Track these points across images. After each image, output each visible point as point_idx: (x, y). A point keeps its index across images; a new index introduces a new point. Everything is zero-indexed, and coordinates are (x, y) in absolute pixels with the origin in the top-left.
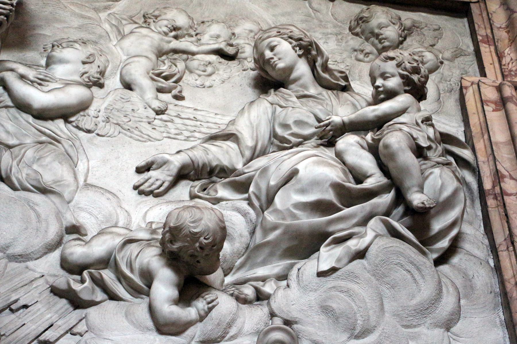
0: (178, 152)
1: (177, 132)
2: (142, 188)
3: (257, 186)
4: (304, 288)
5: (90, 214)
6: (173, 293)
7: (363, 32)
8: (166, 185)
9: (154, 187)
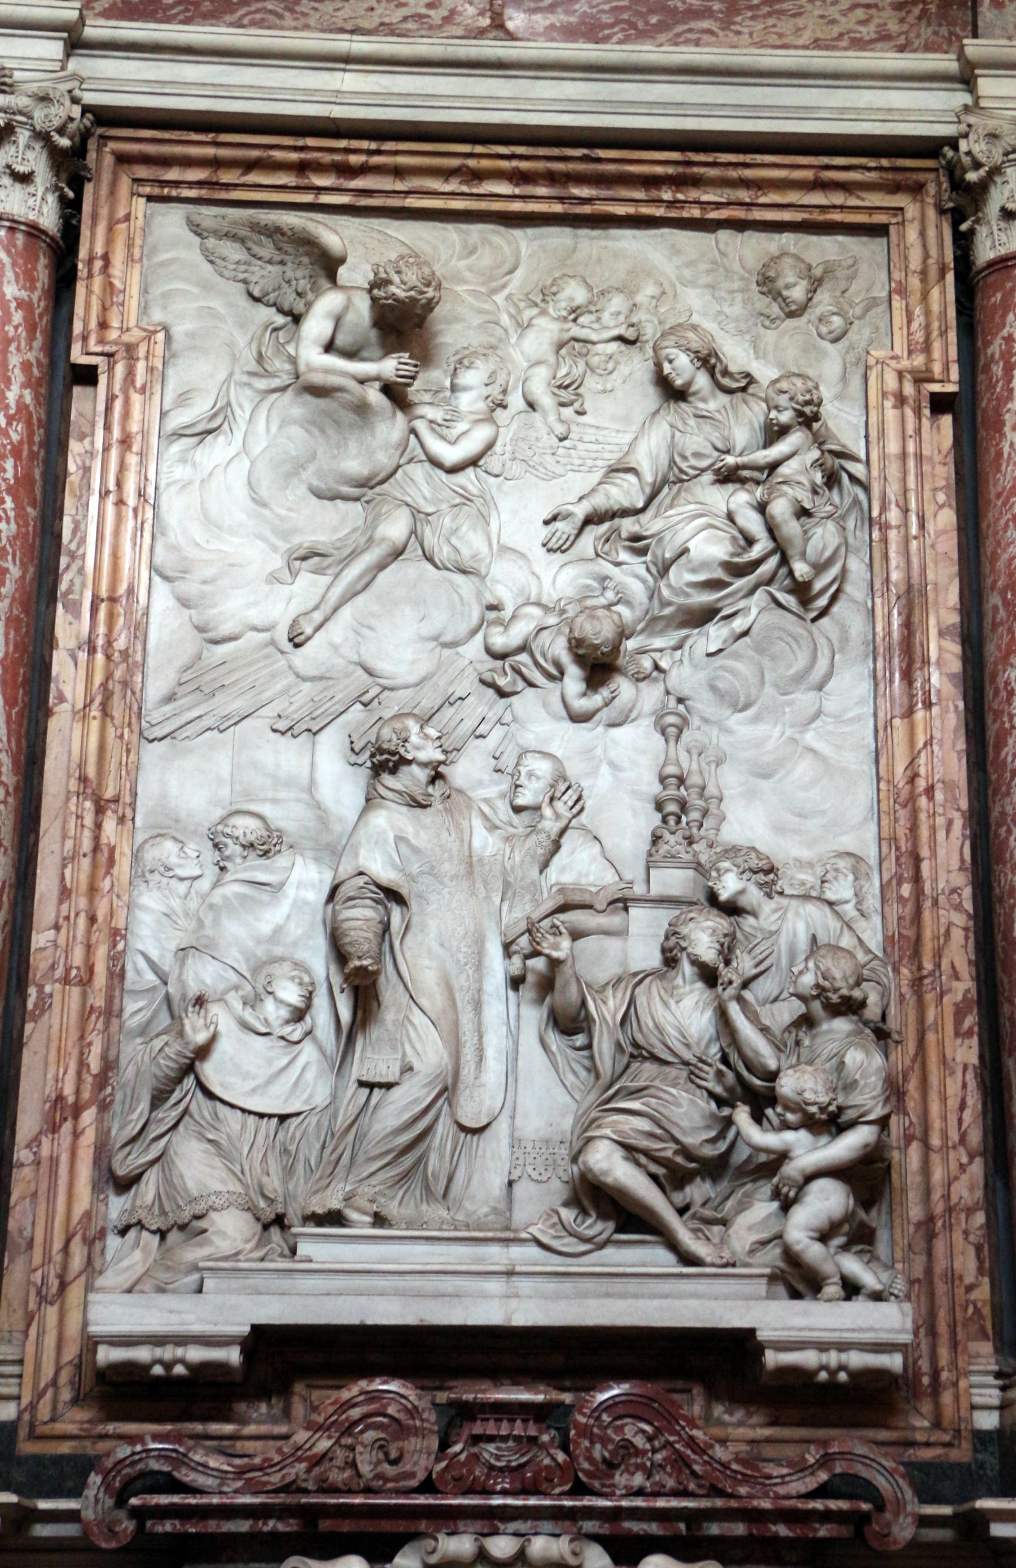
0: (581, 499)
1: (580, 462)
2: (550, 545)
3: (654, 555)
4: (695, 667)
5: (506, 586)
6: (581, 686)
7: (770, 292)
8: (572, 538)
9: (561, 542)
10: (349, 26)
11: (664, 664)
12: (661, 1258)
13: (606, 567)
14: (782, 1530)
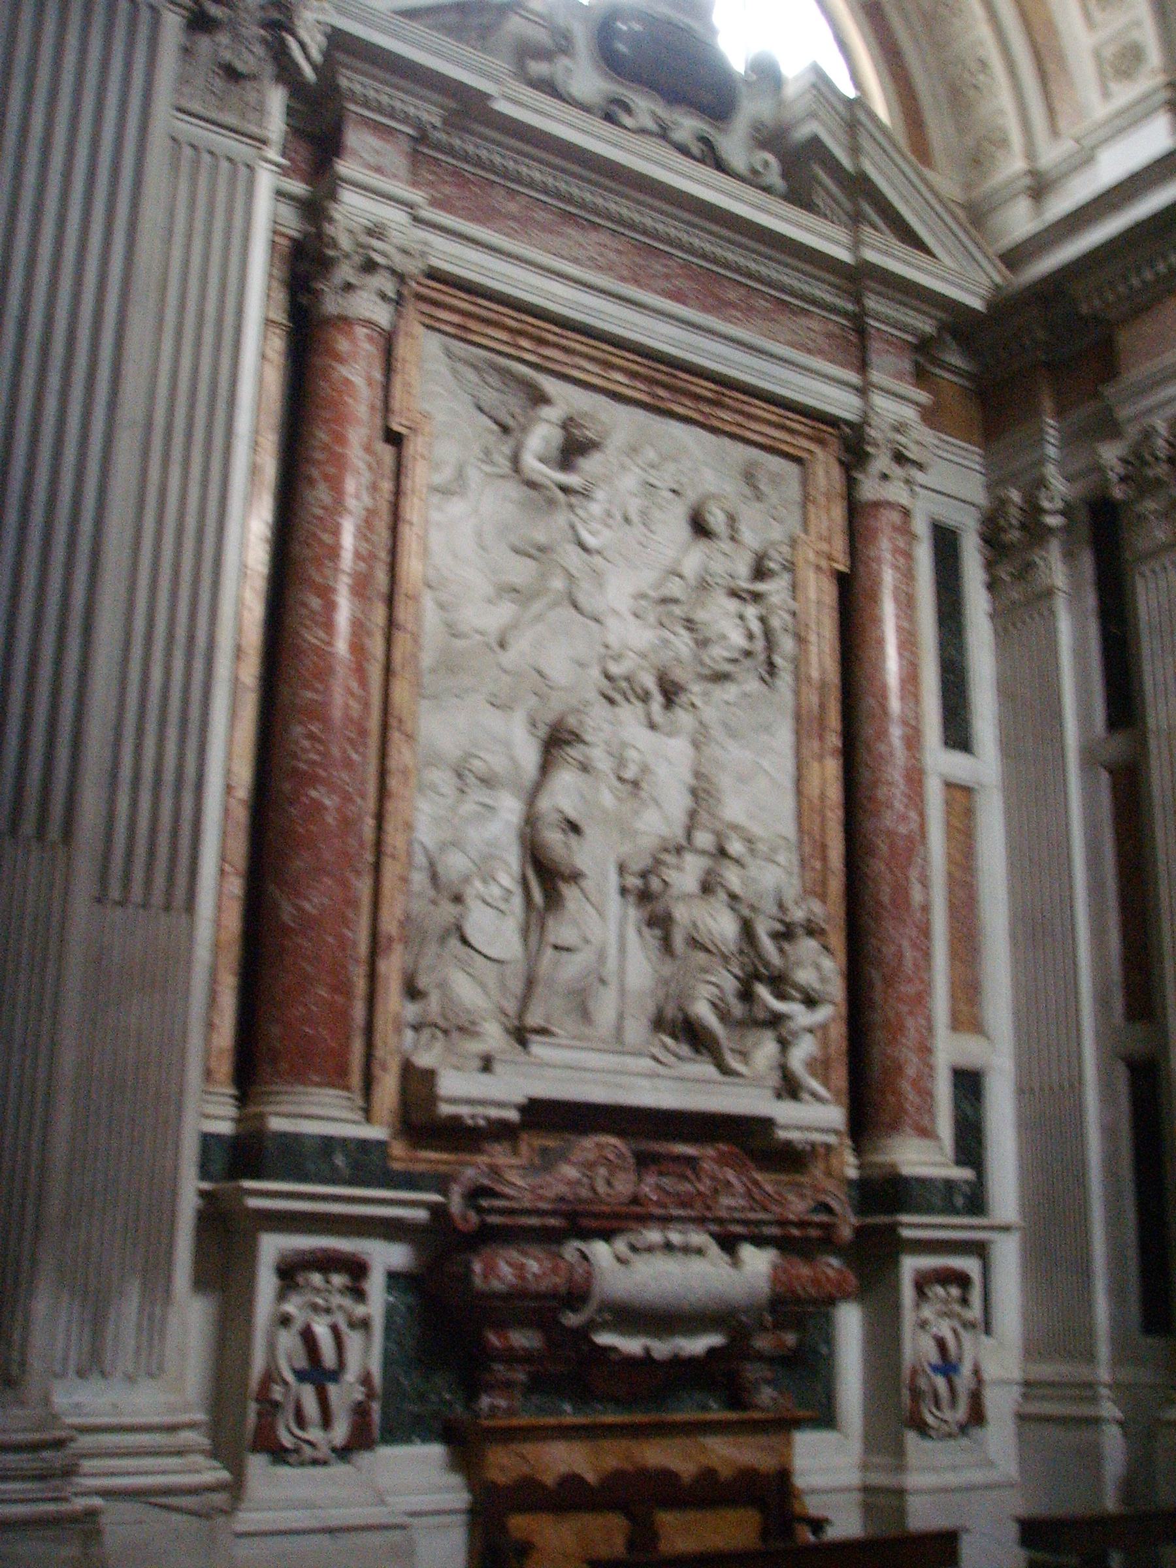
10: (553, 251)
11: (698, 703)
12: (709, 1070)
13: (667, 634)
14: (795, 1232)
